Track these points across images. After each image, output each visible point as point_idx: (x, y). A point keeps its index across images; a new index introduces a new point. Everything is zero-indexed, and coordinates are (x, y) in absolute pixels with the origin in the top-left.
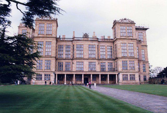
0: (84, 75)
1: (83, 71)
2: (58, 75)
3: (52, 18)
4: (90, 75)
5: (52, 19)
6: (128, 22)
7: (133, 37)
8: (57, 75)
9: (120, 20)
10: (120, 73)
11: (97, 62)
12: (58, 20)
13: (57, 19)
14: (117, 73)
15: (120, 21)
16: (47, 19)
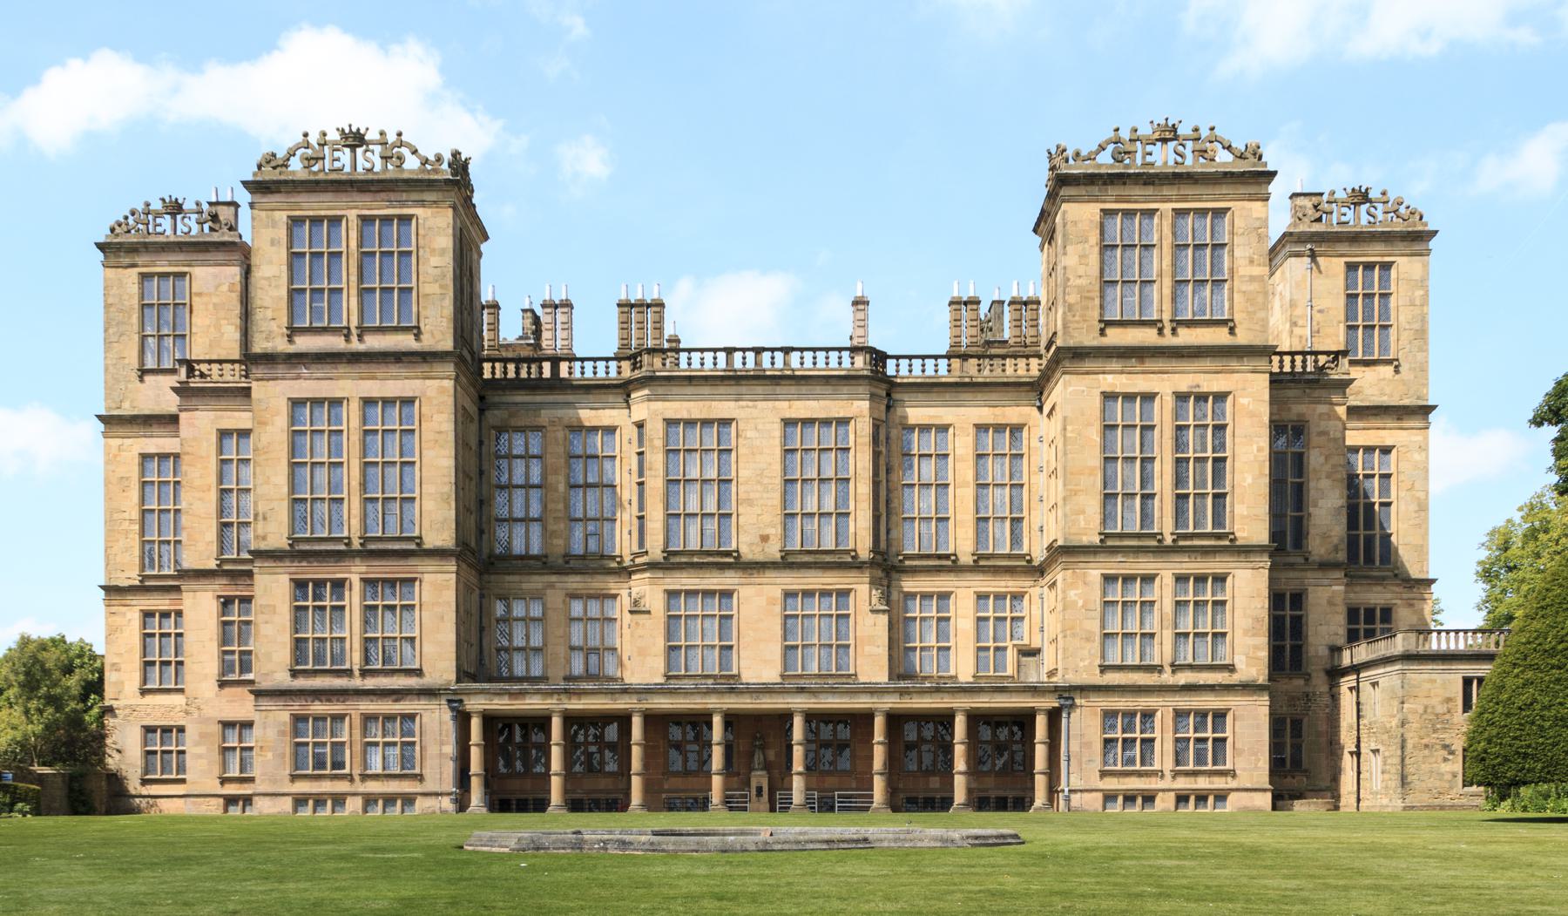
0: (731, 719)
1: (730, 684)
2: (489, 719)
3: (415, 152)
4: (786, 717)
5: (412, 163)
6: (1189, 161)
7: (1229, 324)
8: (476, 724)
9: (1102, 148)
10: (1072, 706)
11: (863, 591)
12: (472, 169)
13: (460, 166)
14: (1051, 702)
15: (1105, 158)
16: (362, 164)
